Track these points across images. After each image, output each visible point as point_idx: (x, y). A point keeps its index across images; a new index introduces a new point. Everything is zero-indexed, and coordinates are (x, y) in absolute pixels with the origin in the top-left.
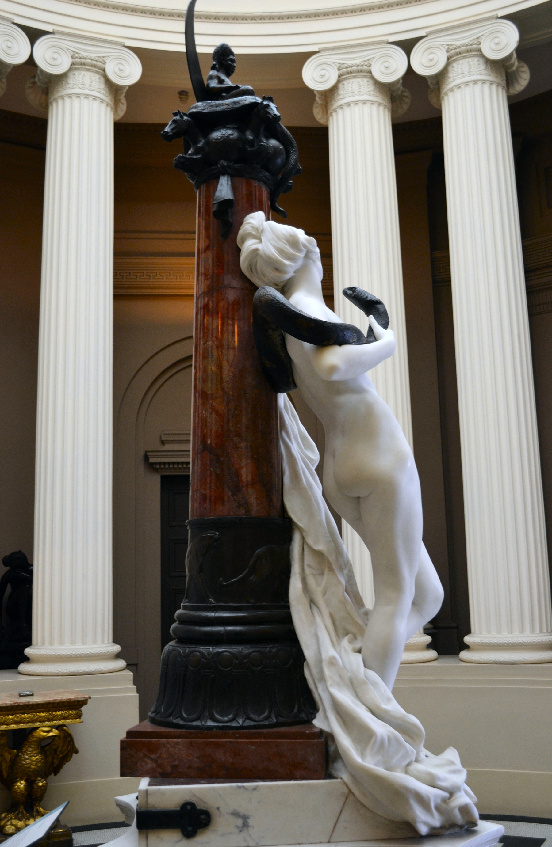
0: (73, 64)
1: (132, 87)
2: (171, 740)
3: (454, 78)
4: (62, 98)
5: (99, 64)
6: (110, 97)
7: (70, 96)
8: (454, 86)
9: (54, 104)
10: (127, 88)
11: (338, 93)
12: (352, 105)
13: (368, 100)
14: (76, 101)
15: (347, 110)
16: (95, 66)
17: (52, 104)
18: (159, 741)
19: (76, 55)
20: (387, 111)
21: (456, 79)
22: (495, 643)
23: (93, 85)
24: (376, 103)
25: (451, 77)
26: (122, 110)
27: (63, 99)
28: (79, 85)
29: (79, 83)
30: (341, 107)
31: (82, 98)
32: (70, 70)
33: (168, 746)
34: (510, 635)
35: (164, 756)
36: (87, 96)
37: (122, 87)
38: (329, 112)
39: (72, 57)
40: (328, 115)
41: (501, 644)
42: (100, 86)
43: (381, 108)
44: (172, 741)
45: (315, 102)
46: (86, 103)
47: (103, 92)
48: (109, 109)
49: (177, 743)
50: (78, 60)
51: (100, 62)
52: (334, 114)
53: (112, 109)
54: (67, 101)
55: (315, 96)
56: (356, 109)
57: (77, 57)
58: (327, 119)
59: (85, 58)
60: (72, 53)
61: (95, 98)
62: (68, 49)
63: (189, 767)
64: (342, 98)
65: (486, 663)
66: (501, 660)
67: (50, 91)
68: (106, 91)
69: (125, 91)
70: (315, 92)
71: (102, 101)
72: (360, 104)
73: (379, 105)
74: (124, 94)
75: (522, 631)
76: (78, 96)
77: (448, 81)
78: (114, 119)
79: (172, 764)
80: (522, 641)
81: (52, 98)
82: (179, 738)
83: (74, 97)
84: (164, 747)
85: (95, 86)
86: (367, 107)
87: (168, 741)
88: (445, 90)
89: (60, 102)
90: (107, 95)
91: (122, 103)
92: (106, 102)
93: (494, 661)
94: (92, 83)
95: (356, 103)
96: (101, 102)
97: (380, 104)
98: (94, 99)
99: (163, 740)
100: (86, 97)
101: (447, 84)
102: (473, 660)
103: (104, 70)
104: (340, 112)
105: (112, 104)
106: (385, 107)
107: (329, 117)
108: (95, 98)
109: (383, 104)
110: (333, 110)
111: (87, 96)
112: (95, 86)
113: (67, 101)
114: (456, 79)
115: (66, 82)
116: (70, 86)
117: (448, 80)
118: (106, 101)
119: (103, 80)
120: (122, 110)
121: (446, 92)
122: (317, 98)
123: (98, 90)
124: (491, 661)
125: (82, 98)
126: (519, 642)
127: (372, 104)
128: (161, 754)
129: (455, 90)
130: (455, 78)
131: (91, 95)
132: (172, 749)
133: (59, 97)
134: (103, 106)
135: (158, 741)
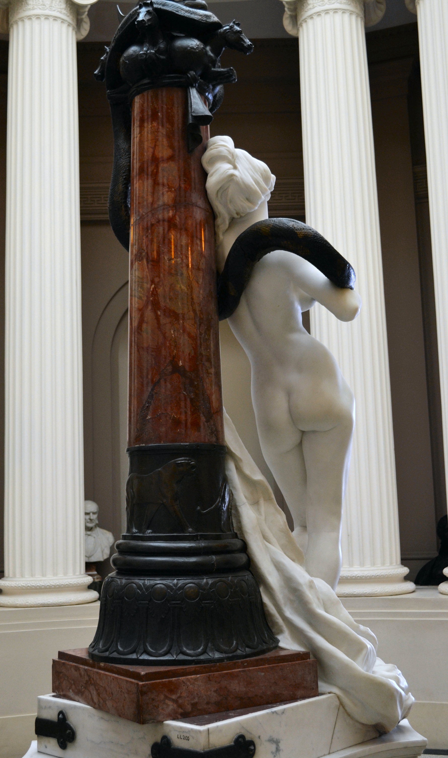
1: (93, 6)
2: (190, 677)
3: (314, 5)
4: (22, 20)
6: (71, 17)
7: (30, 18)
8: (314, 13)
9: (15, 27)
10: (89, 6)
11: (307, 3)
12: (323, 14)
13: (340, 9)
14: (36, 23)
15: (317, 20)
17: (12, 27)
18: (179, 679)
20: (359, 20)
21: (316, 6)
22: (43, 585)
23: (53, 5)
24: (348, 11)
25: (311, 4)
26: (86, 30)
27: (23, 21)
28: (39, 5)
29: (39, 3)
30: (311, 17)
31: (42, 19)
33: (188, 683)
34: (55, 578)
35: (184, 695)
36: (47, 17)
37: (84, 6)
38: (299, 23)
40: (298, 26)
41: (38, 587)
42: (61, 5)
43: (354, 17)
44: (191, 678)
45: (285, 13)
46: (46, 24)
47: (64, 11)
48: (71, 29)
49: (196, 680)
52: (304, 25)
53: (73, 29)
54: (27, 22)
55: (283, 6)
56: (327, 18)
58: (298, 30)
61: (56, 18)
63: (208, 703)
64: (312, 7)
65: (32, 606)
66: (49, 603)
67: (10, 13)
68: (67, 11)
69: (87, 9)
70: (284, 3)
71: (63, 21)
72: (331, 13)
73: (351, 14)
74: (86, 13)
75: (66, 573)
76: (38, 17)
77: (307, 8)
78: (77, 39)
79: (192, 702)
80: (68, 582)
81: (12, 20)
82: (197, 674)
83: (34, 19)
84: (184, 686)
85: (56, 6)
86: (338, 17)
87: (187, 679)
88: (304, 17)
89: (20, 23)
90: (68, 15)
91: (85, 22)
92: (67, 22)
93: (41, 604)
94: (52, 3)
95: (327, 12)
96: (62, 22)
97: (351, 13)
98: (54, 20)
99: (183, 678)
100: (46, 18)
101: (306, 10)
102: (18, 604)
104: (310, 22)
105: (74, 23)
106: (357, 16)
107: (299, 28)
108: (56, 18)
109: (355, 12)
110: (303, 21)
111: (47, 17)
112: (56, 6)
113: (27, 22)
114: (316, 6)
115: (25, 3)
116: (30, 7)
117: (307, 7)
118: (67, 21)
120: (86, 30)
121: (305, 19)
122: (286, 9)
123: (59, 10)
124: (39, 605)
125: (42, 19)
126: (66, 583)
127: (343, 12)
128: (181, 693)
129: (315, 17)
130: (315, 5)
131: (51, 16)
132: (191, 686)
133: (19, 19)
134: (65, 26)
135: (178, 679)
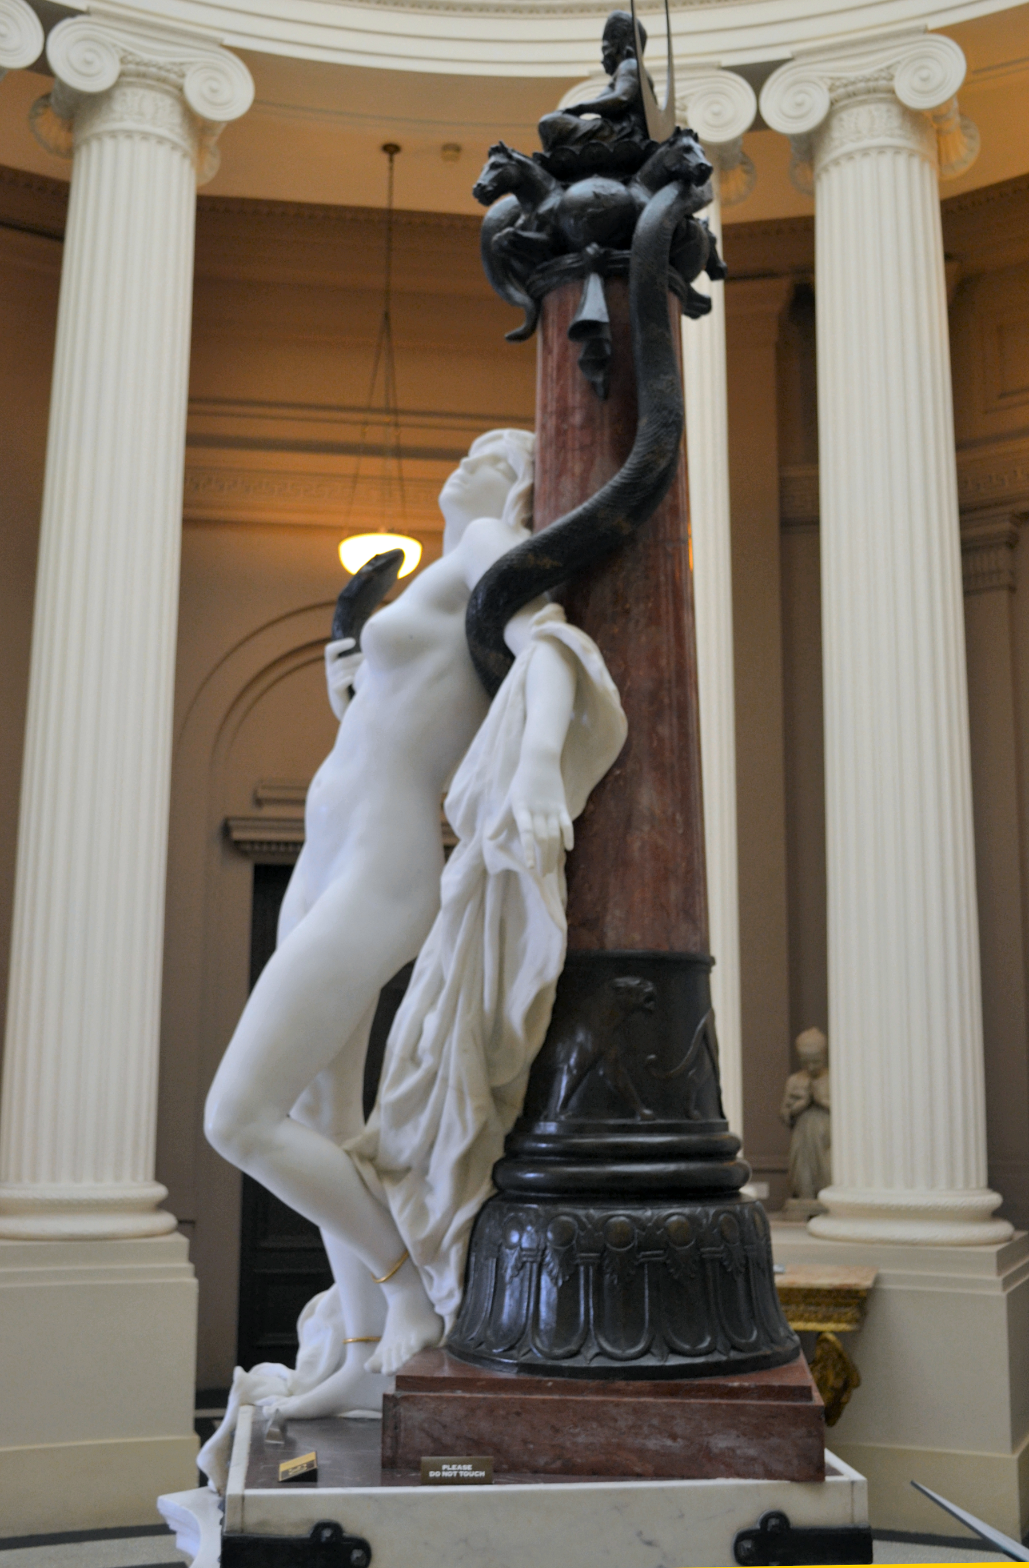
0: (122, 74)
5: (173, 77)
10: (223, 126)
16: (164, 81)
19: (130, 58)
32: (117, 85)
39: (123, 61)
47: (178, 130)
50: (132, 67)
51: (175, 73)
57: (130, 62)
59: (146, 65)
60: (122, 54)
62: (114, 46)
69: (219, 131)
103: (181, 89)
119: (178, 109)
